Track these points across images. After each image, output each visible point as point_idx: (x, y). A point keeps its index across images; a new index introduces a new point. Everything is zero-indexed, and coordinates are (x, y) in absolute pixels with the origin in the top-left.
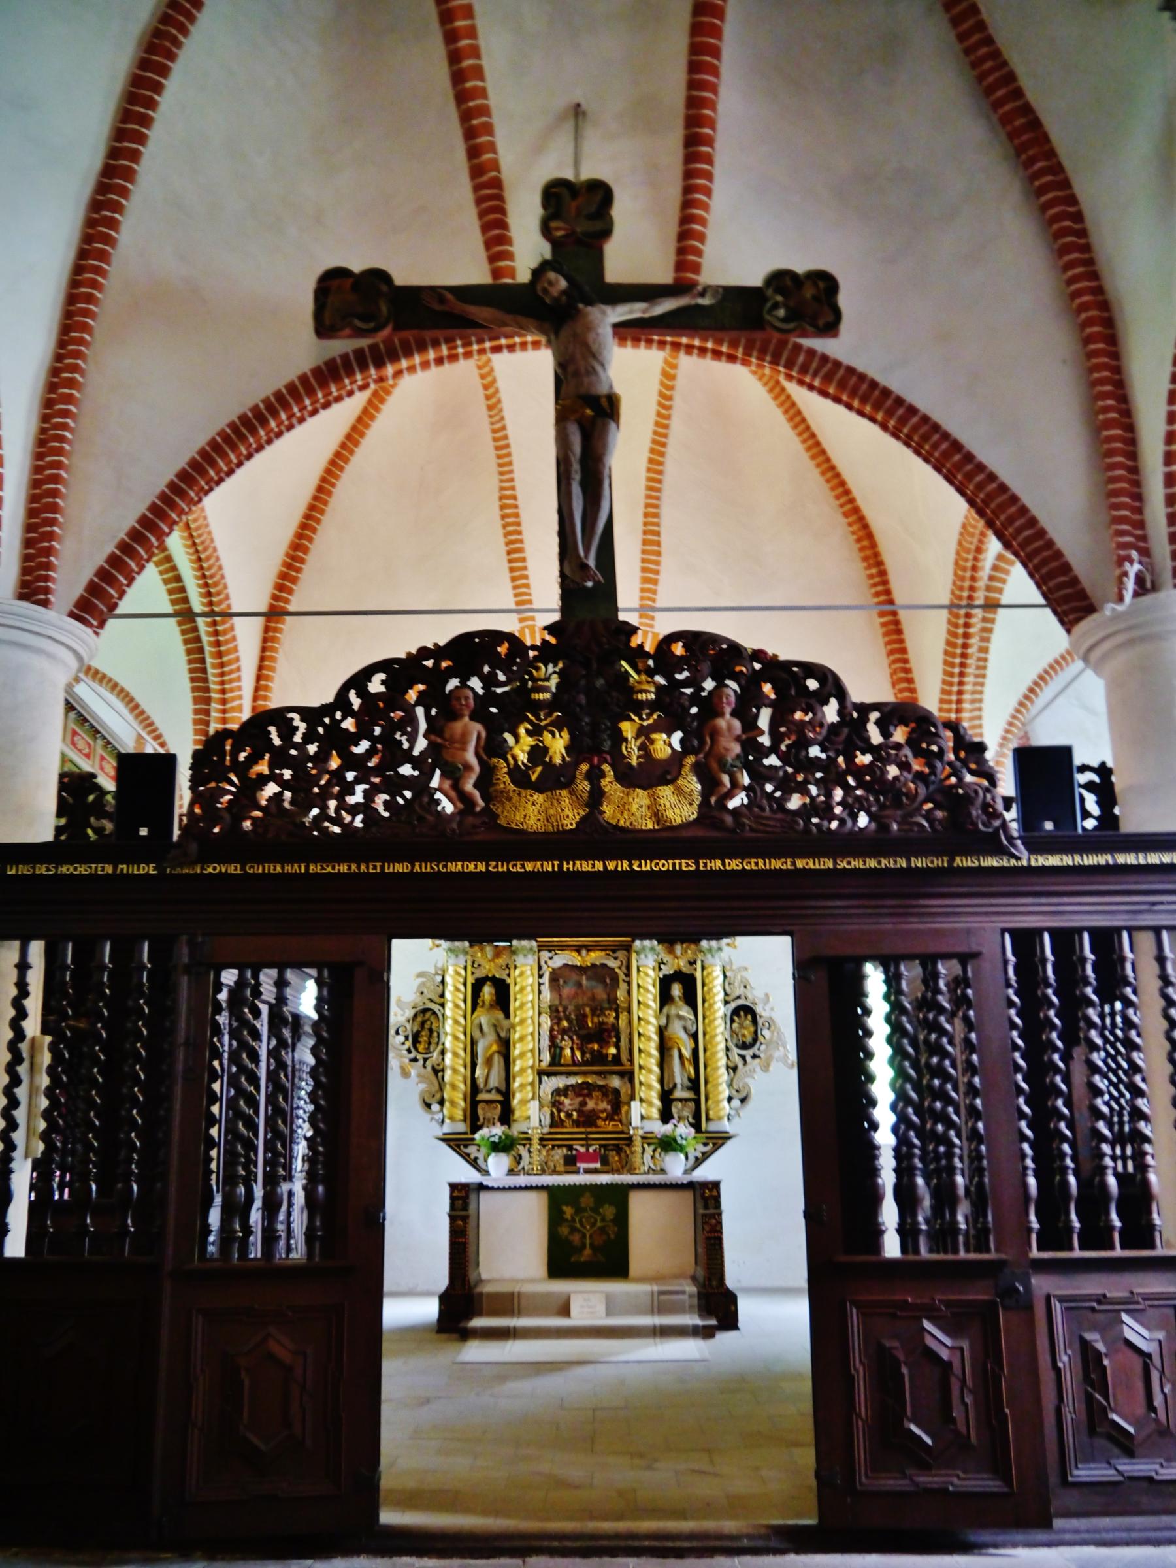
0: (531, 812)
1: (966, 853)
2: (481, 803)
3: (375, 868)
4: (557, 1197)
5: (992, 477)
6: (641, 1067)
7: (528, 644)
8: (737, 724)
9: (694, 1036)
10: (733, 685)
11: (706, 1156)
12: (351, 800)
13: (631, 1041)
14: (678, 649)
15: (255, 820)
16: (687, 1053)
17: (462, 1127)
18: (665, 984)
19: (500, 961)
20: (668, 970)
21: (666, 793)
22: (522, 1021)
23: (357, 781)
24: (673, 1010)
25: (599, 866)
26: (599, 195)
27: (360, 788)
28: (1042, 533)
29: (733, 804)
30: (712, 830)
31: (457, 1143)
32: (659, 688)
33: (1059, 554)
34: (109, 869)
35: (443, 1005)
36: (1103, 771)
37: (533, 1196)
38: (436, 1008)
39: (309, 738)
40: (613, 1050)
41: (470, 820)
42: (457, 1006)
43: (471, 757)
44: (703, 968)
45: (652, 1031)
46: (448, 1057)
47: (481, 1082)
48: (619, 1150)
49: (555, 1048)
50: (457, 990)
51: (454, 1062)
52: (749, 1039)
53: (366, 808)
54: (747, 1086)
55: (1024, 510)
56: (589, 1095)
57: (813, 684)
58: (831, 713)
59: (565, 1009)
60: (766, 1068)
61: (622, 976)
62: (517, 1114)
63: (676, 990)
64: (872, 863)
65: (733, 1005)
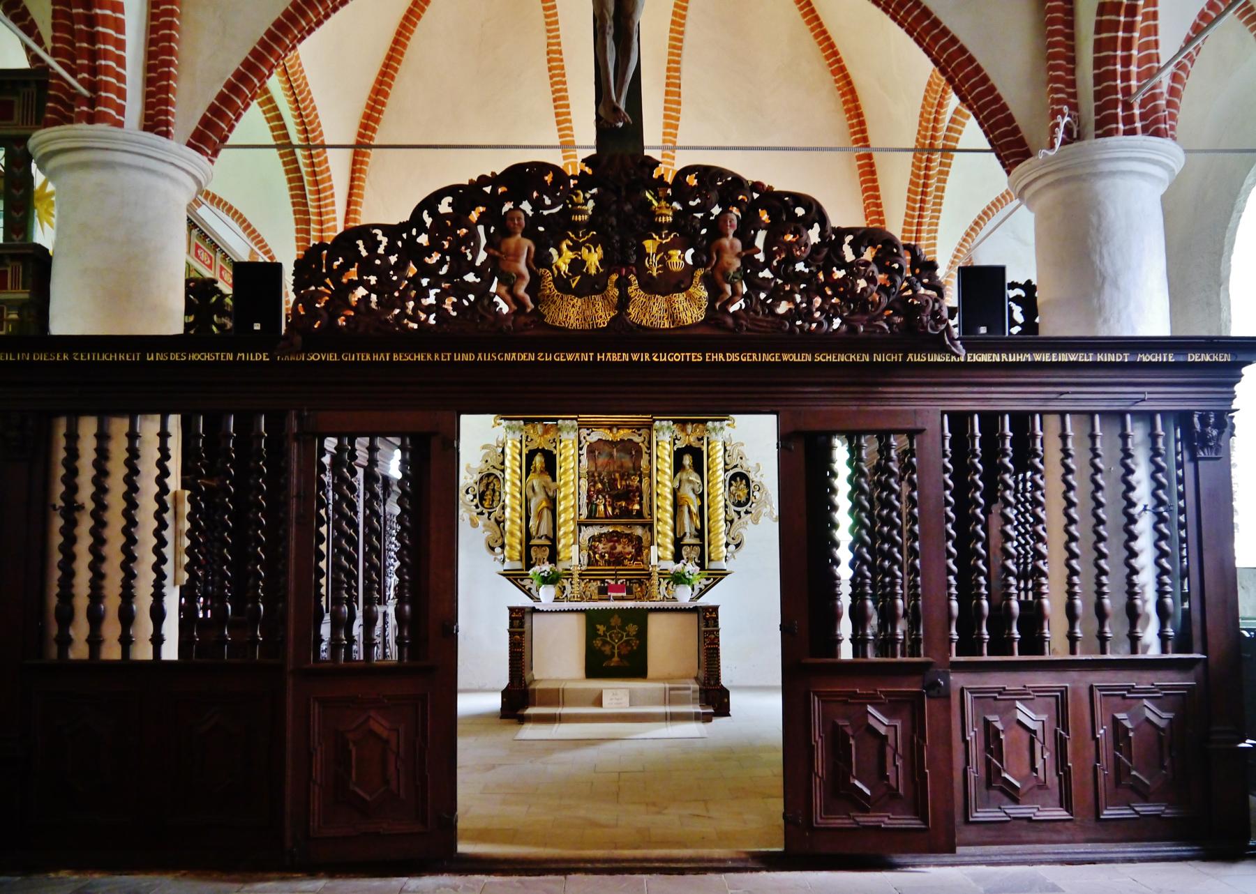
0: (571, 313)
1: (917, 350)
2: (531, 306)
3: (446, 357)
4: (593, 618)
5: (954, 40)
6: (658, 520)
7: (570, 173)
8: (738, 243)
9: (701, 496)
10: (735, 210)
11: (708, 588)
12: (426, 302)
13: (651, 499)
14: (692, 180)
15: (348, 319)
16: (695, 509)
17: (518, 565)
18: (678, 455)
19: (548, 437)
20: (680, 445)
21: (680, 298)
22: (566, 484)
23: (430, 286)
24: (684, 477)
25: (626, 357)
27: (432, 292)
28: (992, 89)
29: (733, 308)
30: (716, 329)
31: (514, 577)
32: (676, 212)
33: (1004, 108)
34: (230, 357)
35: (503, 471)
36: (1029, 287)
37: (574, 616)
38: (498, 473)
39: (390, 250)
40: (637, 507)
41: (522, 319)
42: (514, 471)
43: (522, 267)
44: (708, 444)
45: (667, 492)
46: (508, 511)
47: (533, 531)
48: (640, 583)
49: (590, 502)
50: (514, 458)
51: (513, 514)
52: (743, 499)
53: (438, 308)
54: (741, 534)
55: (978, 69)
56: (618, 541)
57: (800, 211)
58: (814, 235)
59: (600, 475)
60: (756, 522)
61: (645, 449)
62: (562, 555)
63: (687, 460)
64: (842, 358)
65: (731, 472)
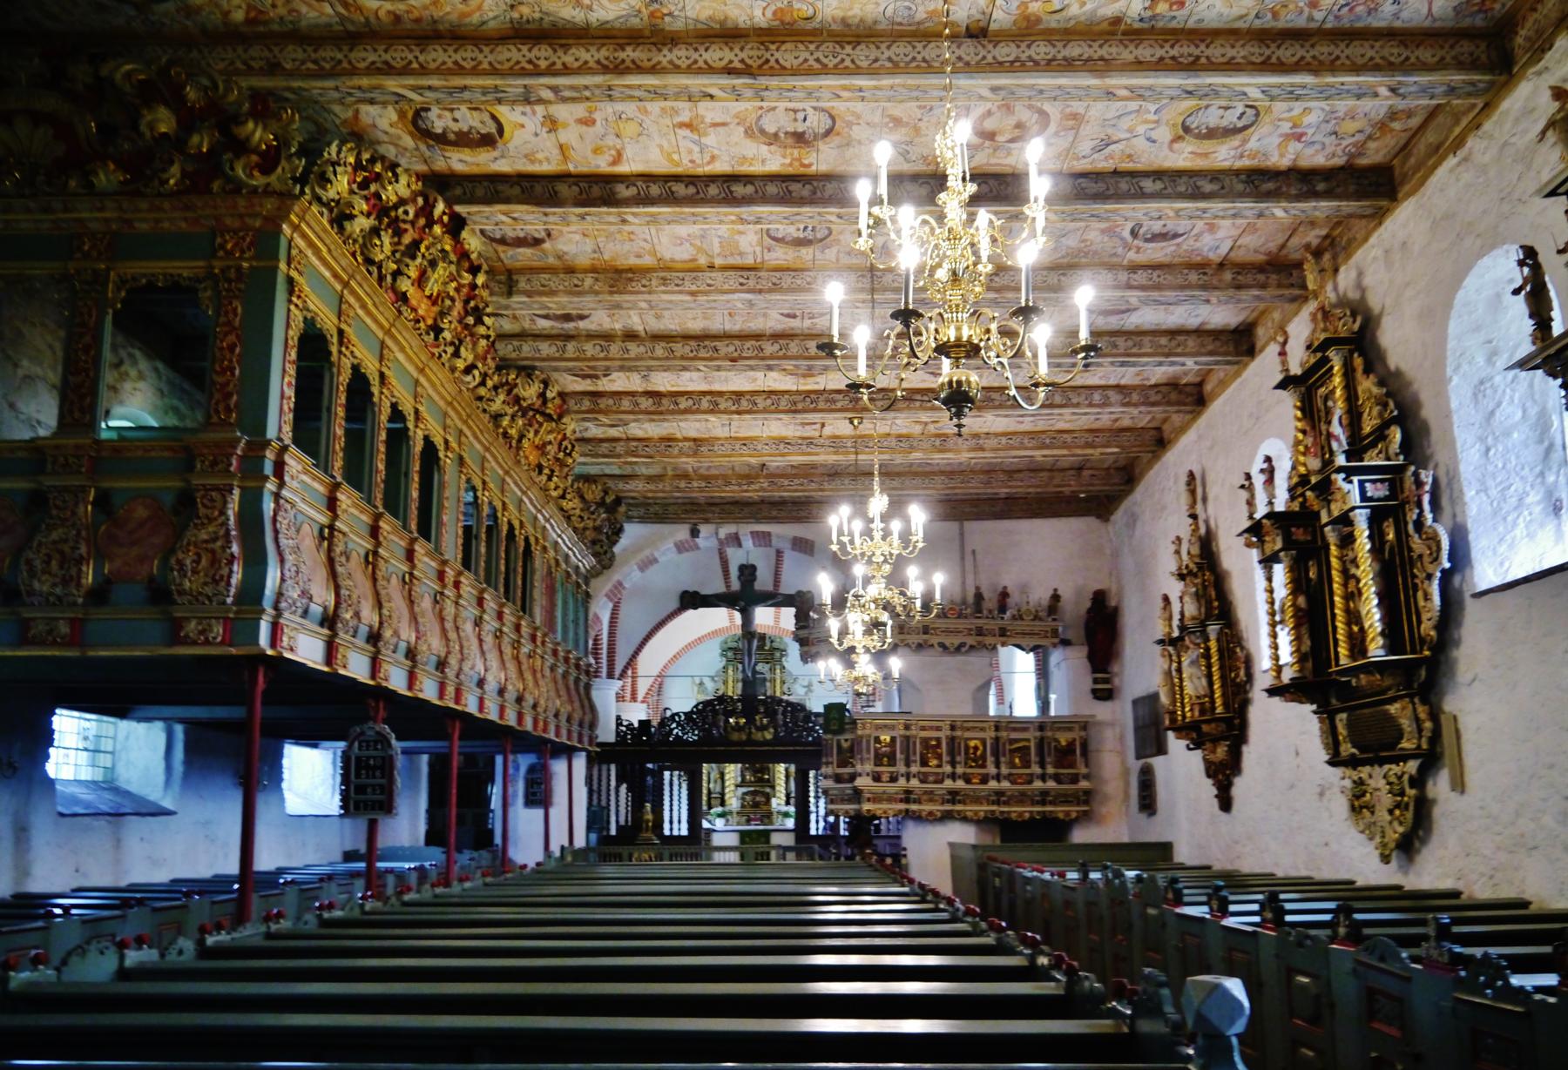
0: (735, 736)
26: (753, 568)
30: (777, 740)
49: (743, 776)
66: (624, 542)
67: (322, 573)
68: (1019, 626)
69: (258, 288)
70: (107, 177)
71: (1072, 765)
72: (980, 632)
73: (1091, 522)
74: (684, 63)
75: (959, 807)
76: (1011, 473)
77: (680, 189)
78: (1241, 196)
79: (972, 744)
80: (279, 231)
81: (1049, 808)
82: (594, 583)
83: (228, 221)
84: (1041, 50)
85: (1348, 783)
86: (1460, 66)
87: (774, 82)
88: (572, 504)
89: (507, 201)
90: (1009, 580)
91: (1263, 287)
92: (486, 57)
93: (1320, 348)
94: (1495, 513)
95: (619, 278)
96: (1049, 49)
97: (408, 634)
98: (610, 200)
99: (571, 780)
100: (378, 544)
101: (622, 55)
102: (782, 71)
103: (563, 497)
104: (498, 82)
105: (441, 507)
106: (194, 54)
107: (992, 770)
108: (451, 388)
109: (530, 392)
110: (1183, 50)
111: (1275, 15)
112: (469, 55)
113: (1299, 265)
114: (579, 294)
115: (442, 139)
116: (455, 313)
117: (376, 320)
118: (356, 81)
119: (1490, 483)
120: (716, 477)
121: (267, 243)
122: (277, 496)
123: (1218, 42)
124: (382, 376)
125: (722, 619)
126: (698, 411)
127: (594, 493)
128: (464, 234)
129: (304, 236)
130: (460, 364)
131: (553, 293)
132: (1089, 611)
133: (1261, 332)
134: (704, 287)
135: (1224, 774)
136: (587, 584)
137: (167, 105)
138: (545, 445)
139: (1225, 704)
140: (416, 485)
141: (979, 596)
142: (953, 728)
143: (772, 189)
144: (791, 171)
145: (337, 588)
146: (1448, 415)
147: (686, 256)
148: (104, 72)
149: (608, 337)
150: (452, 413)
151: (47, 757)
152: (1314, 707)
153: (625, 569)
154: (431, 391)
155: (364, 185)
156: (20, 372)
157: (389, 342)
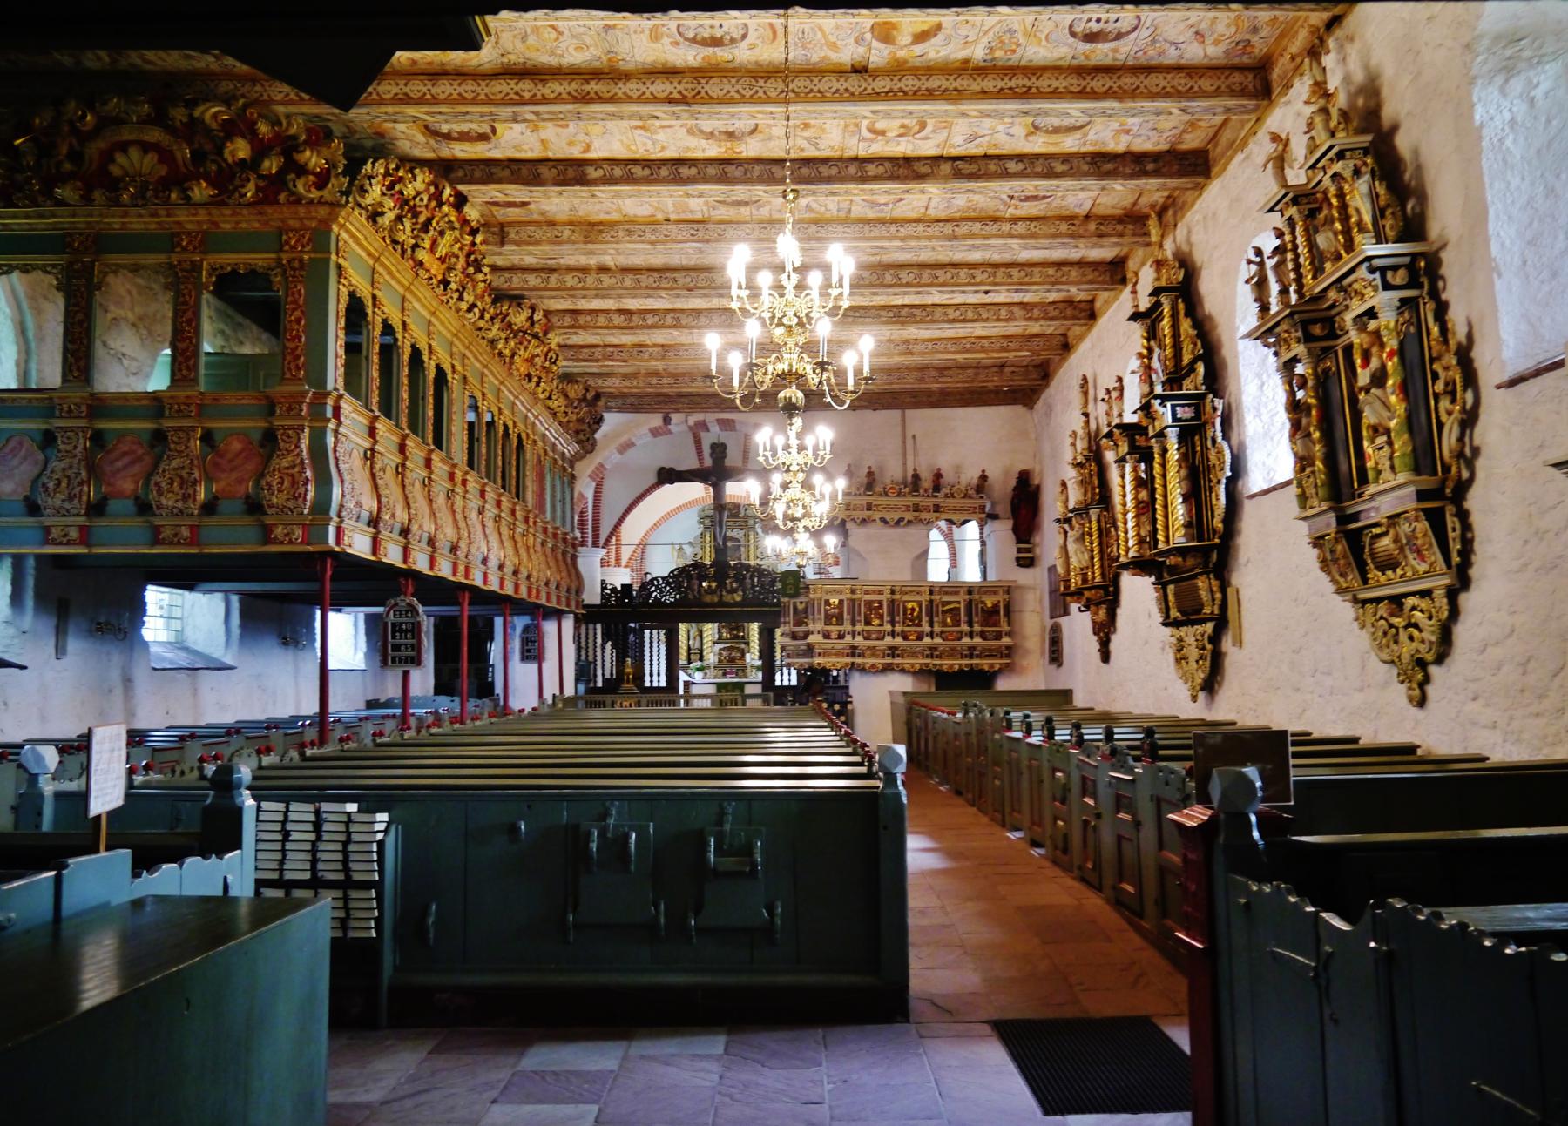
0: (708, 599)
66: (604, 428)
67: (368, 486)
68: (951, 503)
69: (317, 273)
70: (201, 191)
71: (996, 624)
72: (917, 508)
73: (1019, 409)
74: (635, 95)
75: (897, 660)
76: (942, 370)
77: (638, 171)
78: (1086, 175)
79: (910, 606)
80: (330, 230)
81: (975, 661)
82: (578, 465)
83: (291, 222)
84: (909, 83)
85: (1174, 640)
86: (1232, 93)
87: (704, 108)
88: (558, 403)
89: (500, 181)
90: (945, 463)
91: (1121, 235)
92: (484, 89)
93: (1156, 292)
94: (1266, 434)
95: (592, 230)
96: (916, 82)
97: (429, 527)
98: (582, 181)
99: (560, 638)
100: (406, 458)
101: (587, 88)
102: (711, 100)
103: (550, 398)
104: (493, 109)
105: (450, 420)
106: (258, 88)
107: (926, 628)
108: (456, 324)
109: (519, 319)
110: (1018, 82)
111: (1087, 57)
112: (469, 88)
113: (1147, 217)
114: (559, 243)
115: (448, 137)
116: (459, 267)
117: (399, 282)
118: (384, 109)
119: (1263, 410)
120: (683, 375)
121: (321, 239)
122: (336, 432)
123: (1046, 75)
124: (404, 324)
125: (697, 491)
126: (663, 327)
127: (575, 391)
128: (466, 209)
129: (348, 231)
130: (464, 306)
131: (537, 243)
132: (1015, 489)
133: (1131, 265)
134: (662, 238)
135: (1104, 631)
136: (572, 467)
137: (244, 137)
138: (534, 357)
139: (1103, 575)
140: (431, 406)
141: (916, 477)
142: (893, 592)
143: (712, 171)
144: (726, 156)
145: (379, 497)
146: (1236, 357)
147: (646, 213)
148: (197, 113)
149: (584, 270)
150: (456, 342)
151: (143, 623)
152: (1153, 579)
153: (606, 453)
154: (440, 328)
155: (391, 187)
156: (109, 316)
157: (408, 296)
